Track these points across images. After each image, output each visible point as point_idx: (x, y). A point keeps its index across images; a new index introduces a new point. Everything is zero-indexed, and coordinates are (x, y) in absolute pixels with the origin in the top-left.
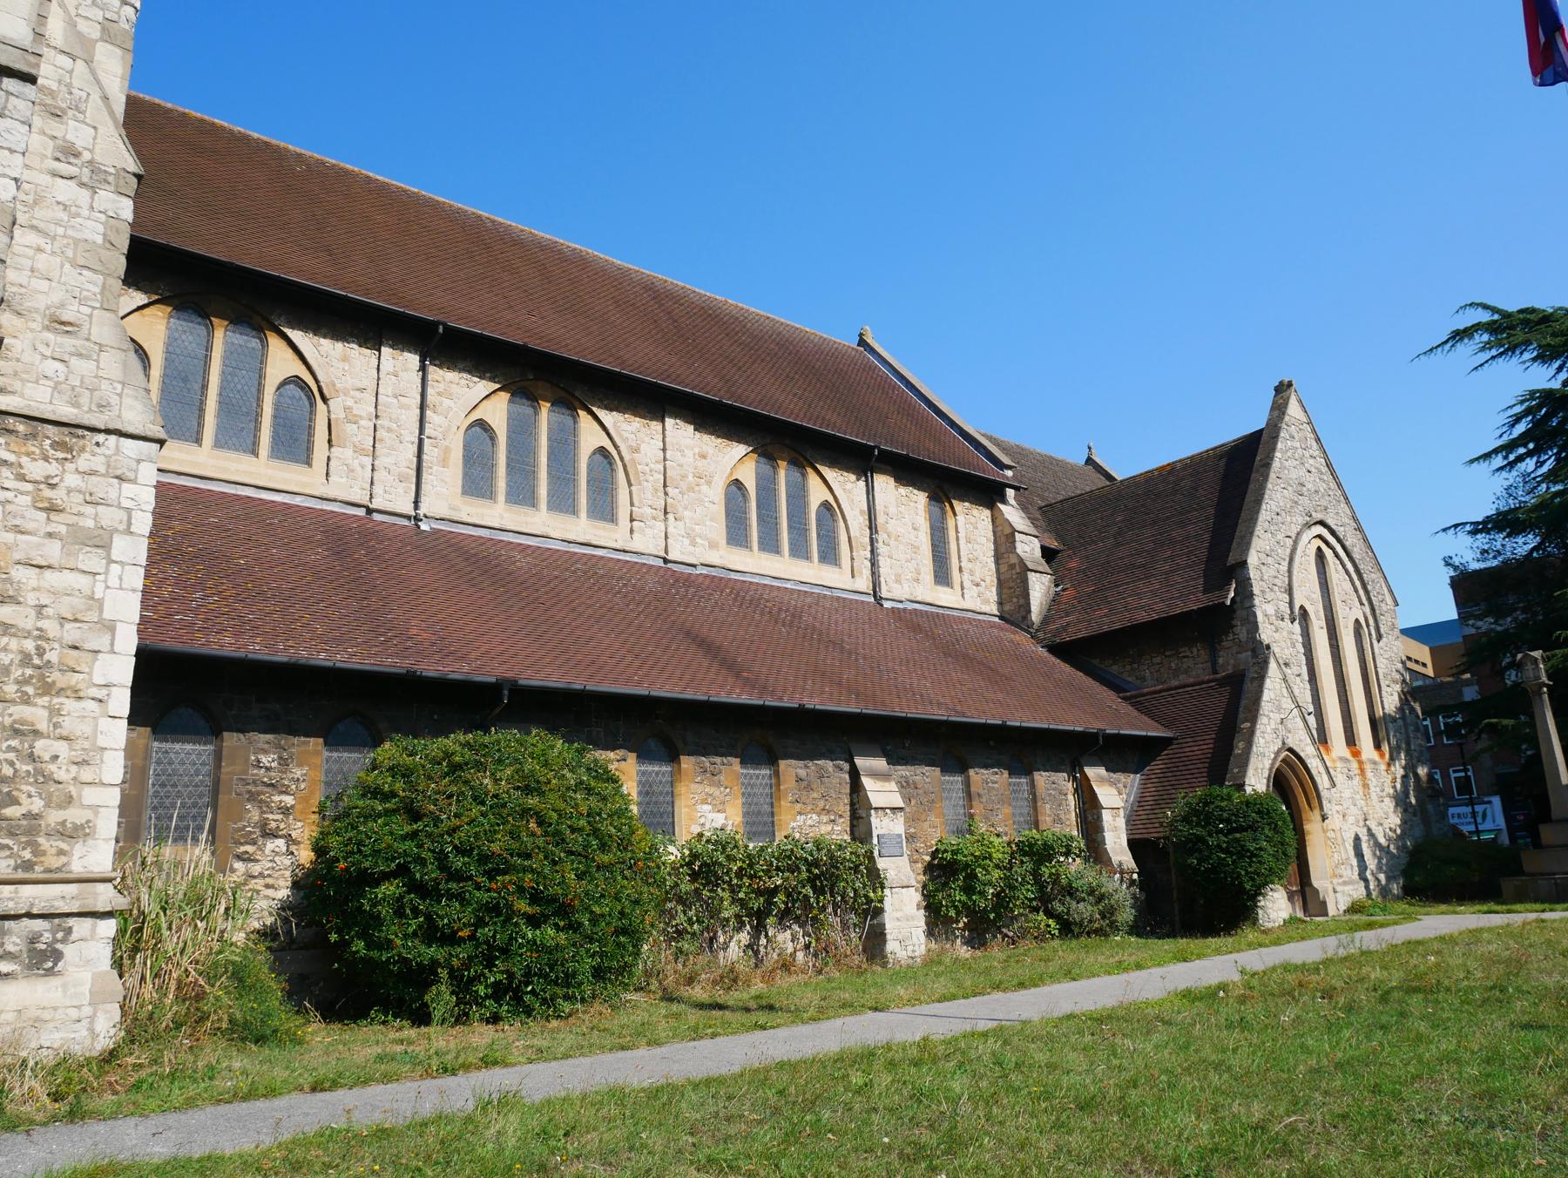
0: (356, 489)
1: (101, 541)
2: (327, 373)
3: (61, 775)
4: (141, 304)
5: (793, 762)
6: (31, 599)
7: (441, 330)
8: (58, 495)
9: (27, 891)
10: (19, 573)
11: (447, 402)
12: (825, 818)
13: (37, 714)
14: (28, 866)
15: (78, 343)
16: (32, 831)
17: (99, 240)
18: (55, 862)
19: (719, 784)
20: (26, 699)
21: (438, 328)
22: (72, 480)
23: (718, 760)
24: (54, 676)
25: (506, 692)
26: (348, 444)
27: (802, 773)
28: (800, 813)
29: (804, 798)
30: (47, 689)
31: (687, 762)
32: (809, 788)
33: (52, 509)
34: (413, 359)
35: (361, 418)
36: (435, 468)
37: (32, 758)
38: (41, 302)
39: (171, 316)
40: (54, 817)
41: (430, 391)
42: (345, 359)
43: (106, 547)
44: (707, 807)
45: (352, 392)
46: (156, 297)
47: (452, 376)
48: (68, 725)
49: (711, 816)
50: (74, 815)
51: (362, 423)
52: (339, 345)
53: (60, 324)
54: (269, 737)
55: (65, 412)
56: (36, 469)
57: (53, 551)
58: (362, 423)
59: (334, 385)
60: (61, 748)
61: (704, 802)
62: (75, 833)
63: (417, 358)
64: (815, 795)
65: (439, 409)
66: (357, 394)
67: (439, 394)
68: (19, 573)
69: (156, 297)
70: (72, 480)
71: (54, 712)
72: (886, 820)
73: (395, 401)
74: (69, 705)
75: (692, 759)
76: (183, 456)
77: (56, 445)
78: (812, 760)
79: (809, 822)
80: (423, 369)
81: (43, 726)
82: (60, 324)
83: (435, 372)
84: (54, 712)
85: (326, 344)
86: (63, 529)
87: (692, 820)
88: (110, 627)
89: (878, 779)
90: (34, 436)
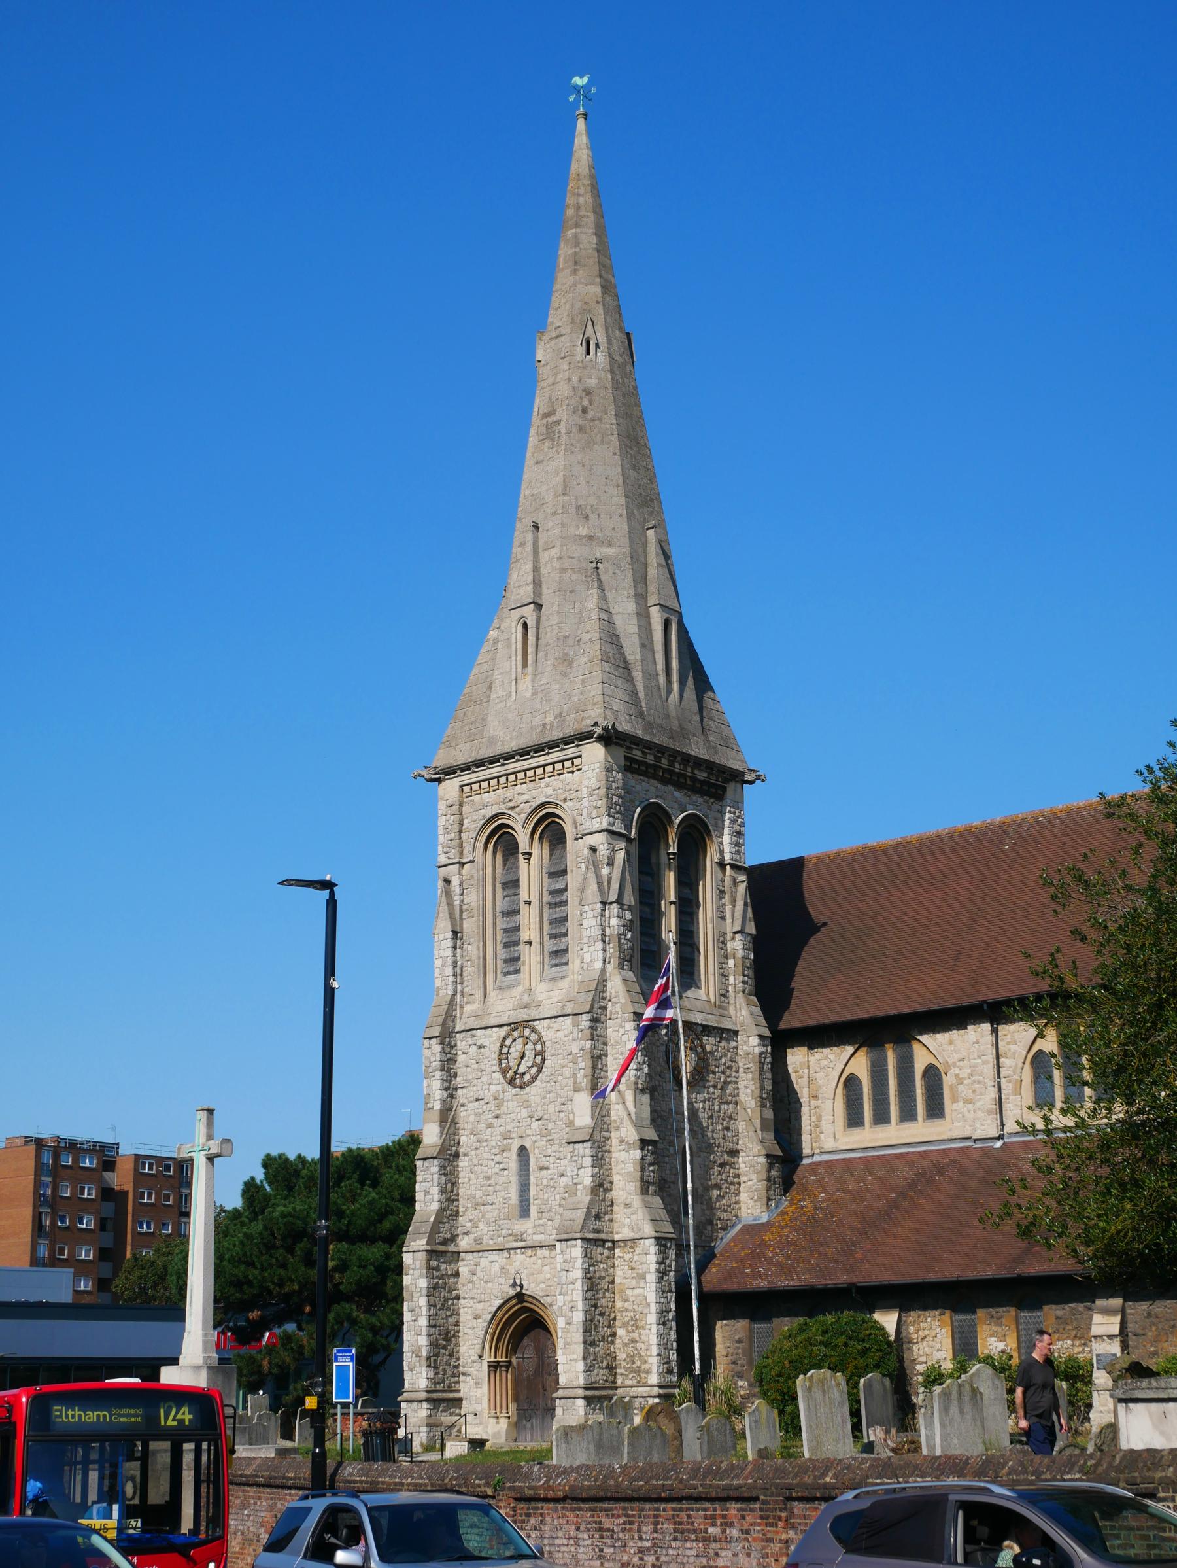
0: (968, 1127)
1: (642, 1277)
2: (943, 1057)
3: (643, 1354)
4: (851, 1052)
5: (1054, 1306)
6: (631, 1299)
7: (985, 1006)
8: (633, 1264)
9: (640, 1389)
10: (629, 1292)
11: (1013, 1048)
12: (1077, 1343)
13: (635, 1335)
14: (639, 1382)
15: (631, 1209)
16: (639, 1371)
17: (632, 1169)
18: (644, 1381)
19: (1001, 1325)
20: (634, 1332)
21: (983, 1007)
22: (636, 1258)
23: (1001, 1309)
24: (638, 1323)
25: (854, 1291)
26: (960, 1099)
27: (1060, 1313)
28: (1059, 1340)
29: (1061, 1330)
30: (637, 1327)
31: (981, 1313)
32: (1066, 1323)
33: (632, 1269)
34: (986, 1027)
35: (965, 1079)
36: (1011, 1097)
37: (637, 1349)
38: (621, 1200)
39: (867, 1053)
40: (643, 1367)
41: (1001, 1044)
42: (951, 1043)
43: (645, 1278)
44: (994, 1339)
45: (958, 1064)
46: (857, 1046)
47: (1012, 1027)
48: (643, 1338)
49: (995, 1344)
50: (646, 1366)
51: (965, 1082)
52: (947, 1035)
53: (627, 1205)
54: (788, 1319)
55: (631, 1235)
56: (627, 1257)
57: (634, 1281)
58: (965, 1082)
59: (947, 1062)
60: (642, 1345)
61: (992, 1336)
62: (648, 1372)
63: (989, 1025)
64: (1070, 1327)
65: (1008, 1055)
66: (961, 1063)
67: (1008, 1043)
68: (629, 1292)
69: (857, 1046)
70: (636, 1258)
71: (640, 1334)
72: (1104, 1344)
73: (979, 1061)
74: (642, 1331)
75: (984, 1310)
76: (881, 1135)
77: (631, 1247)
78: (1067, 1303)
79: (1065, 1346)
80: (995, 1032)
81: (638, 1339)
82: (627, 1205)
83: (1005, 1030)
84: (640, 1334)
85: (939, 1036)
86: (635, 1275)
87: (985, 1347)
88: (648, 1305)
89: (1109, 1315)
90: (626, 1246)
